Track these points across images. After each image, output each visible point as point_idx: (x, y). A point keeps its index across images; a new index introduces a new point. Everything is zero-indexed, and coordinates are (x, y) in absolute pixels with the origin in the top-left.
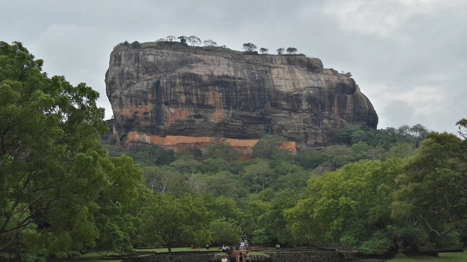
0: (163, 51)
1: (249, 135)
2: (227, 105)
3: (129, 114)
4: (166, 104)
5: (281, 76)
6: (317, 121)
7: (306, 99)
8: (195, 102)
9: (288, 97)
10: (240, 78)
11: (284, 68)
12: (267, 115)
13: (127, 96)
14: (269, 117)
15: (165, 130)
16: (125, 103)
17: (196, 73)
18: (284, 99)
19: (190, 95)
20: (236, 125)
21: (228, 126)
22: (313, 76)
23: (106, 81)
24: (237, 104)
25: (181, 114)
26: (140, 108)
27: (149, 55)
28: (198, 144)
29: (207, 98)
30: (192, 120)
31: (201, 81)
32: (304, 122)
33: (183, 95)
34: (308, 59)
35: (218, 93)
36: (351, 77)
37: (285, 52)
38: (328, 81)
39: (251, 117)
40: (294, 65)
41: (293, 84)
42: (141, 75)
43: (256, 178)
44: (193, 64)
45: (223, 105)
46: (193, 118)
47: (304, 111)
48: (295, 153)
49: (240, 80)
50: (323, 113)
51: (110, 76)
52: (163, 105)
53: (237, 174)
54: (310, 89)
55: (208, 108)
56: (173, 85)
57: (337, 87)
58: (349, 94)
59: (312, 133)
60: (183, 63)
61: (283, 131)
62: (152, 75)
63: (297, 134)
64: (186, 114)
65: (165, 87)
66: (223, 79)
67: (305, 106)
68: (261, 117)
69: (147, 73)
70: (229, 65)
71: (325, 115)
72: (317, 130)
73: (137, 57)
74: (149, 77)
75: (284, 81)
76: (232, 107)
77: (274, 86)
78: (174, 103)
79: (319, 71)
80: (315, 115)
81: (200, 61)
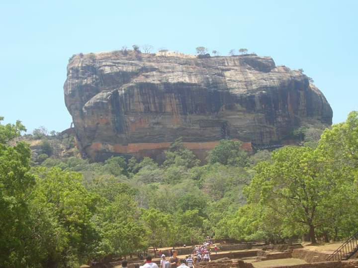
1: (206, 137)
4: (126, 114)
5: (233, 79)
8: (153, 109)
9: (241, 100)
10: (195, 84)
12: (223, 117)
14: (225, 120)
18: (237, 101)
19: (148, 103)
20: (193, 129)
21: (186, 130)
22: (265, 75)
26: (101, 119)
27: (105, 66)
37: (238, 53)
38: (279, 79)
44: (149, 73)
46: (152, 125)
47: (259, 111)
49: (195, 87)
50: (277, 111)
55: (165, 115)
57: (290, 85)
59: (267, 132)
61: (239, 132)
62: (110, 86)
64: (145, 122)
65: (124, 97)
67: (258, 107)
68: (217, 119)
70: (183, 71)
72: (272, 129)
76: (189, 112)
77: (228, 89)
81: (153, 69)
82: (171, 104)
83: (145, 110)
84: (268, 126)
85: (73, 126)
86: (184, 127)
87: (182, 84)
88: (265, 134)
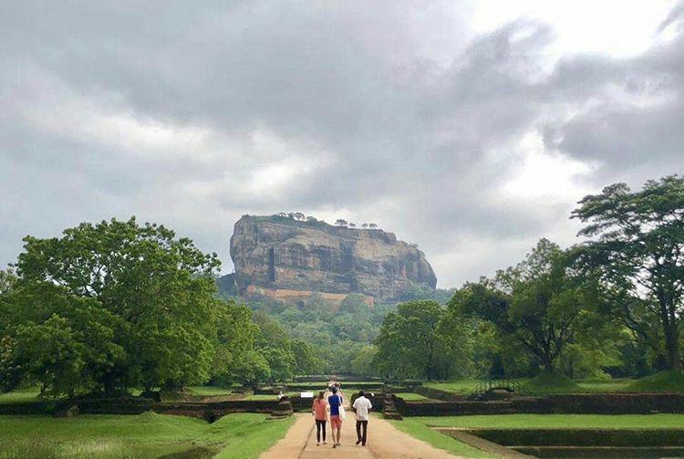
9: (369, 263)
22: (389, 247)
37: (367, 228)
42: (258, 242)
66: (321, 249)
73: (256, 227)
74: (265, 244)
75: (365, 252)
78: (283, 265)
81: (304, 234)
82: (313, 261)
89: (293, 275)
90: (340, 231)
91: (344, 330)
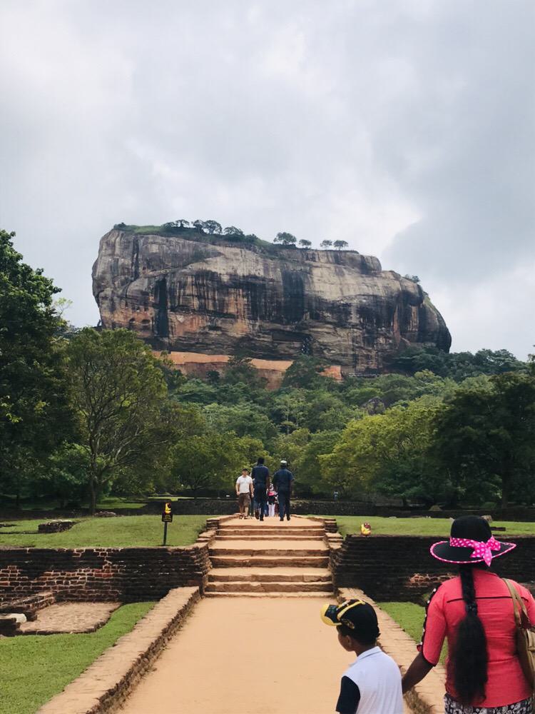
0: (171, 239)
1: (281, 354)
2: (253, 314)
3: (123, 320)
4: (173, 309)
5: (325, 279)
6: (370, 340)
7: (357, 311)
8: (211, 308)
10: (272, 280)
11: (329, 268)
12: (305, 329)
13: (121, 298)
14: (307, 332)
15: (170, 344)
16: (117, 306)
17: (214, 270)
19: (205, 299)
21: (253, 342)
22: (368, 280)
23: (93, 275)
24: (266, 313)
25: (191, 323)
27: (152, 243)
28: (213, 363)
29: (227, 305)
30: (207, 333)
31: (221, 282)
32: (353, 341)
33: (196, 299)
34: (362, 257)
35: (241, 298)
36: (418, 283)
37: (332, 248)
38: (386, 287)
39: (283, 331)
40: (343, 264)
41: (341, 290)
42: (141, 269)
43: (287, 413)
45: (248, 314)
46: (207, 330)
47: (354, 326)
48: (339, 381)
49: (271, 283)
50: (379, 329)
51: (100, 270)
52: (169, 310)
53: (264, 406)
54: (363, 297)
56: (183, 286)
58: (414, 305)
60: (199, 257)
61: (325, 352)
63: (343, 355)
64: (198, 324)
67: (354, 319)
68: (297, 331)
69: (149, 268)
71: (381, 332)
72: (370, 351)
73: (136, 243)
74: (151, 273)
75: (327, 285)
77: (315, 291)
78: (184, 309)
79: (375, 273)
80: (368, 332)
81: (219, 254)
83: (200, 307)
84: (366, 348)
85: (101, 324)
86: (251, 337)
87: (255, 277)
88: (360, 358)
89: (197, 324)
90: (285, 252)
91: (291, 418)
